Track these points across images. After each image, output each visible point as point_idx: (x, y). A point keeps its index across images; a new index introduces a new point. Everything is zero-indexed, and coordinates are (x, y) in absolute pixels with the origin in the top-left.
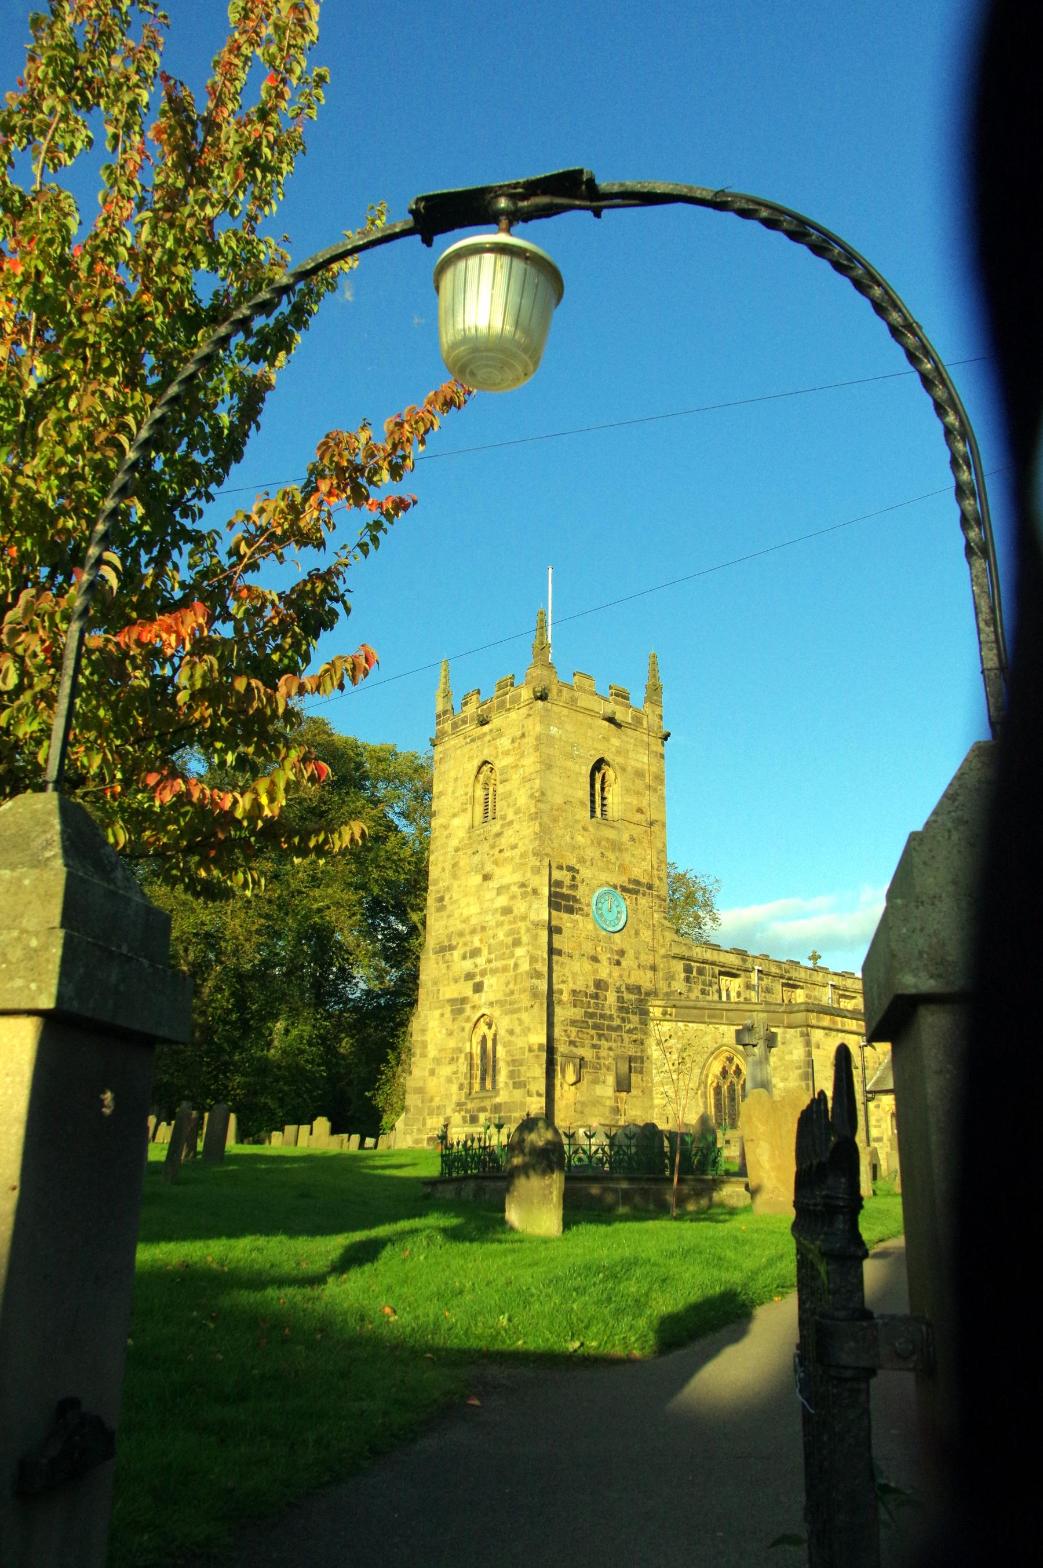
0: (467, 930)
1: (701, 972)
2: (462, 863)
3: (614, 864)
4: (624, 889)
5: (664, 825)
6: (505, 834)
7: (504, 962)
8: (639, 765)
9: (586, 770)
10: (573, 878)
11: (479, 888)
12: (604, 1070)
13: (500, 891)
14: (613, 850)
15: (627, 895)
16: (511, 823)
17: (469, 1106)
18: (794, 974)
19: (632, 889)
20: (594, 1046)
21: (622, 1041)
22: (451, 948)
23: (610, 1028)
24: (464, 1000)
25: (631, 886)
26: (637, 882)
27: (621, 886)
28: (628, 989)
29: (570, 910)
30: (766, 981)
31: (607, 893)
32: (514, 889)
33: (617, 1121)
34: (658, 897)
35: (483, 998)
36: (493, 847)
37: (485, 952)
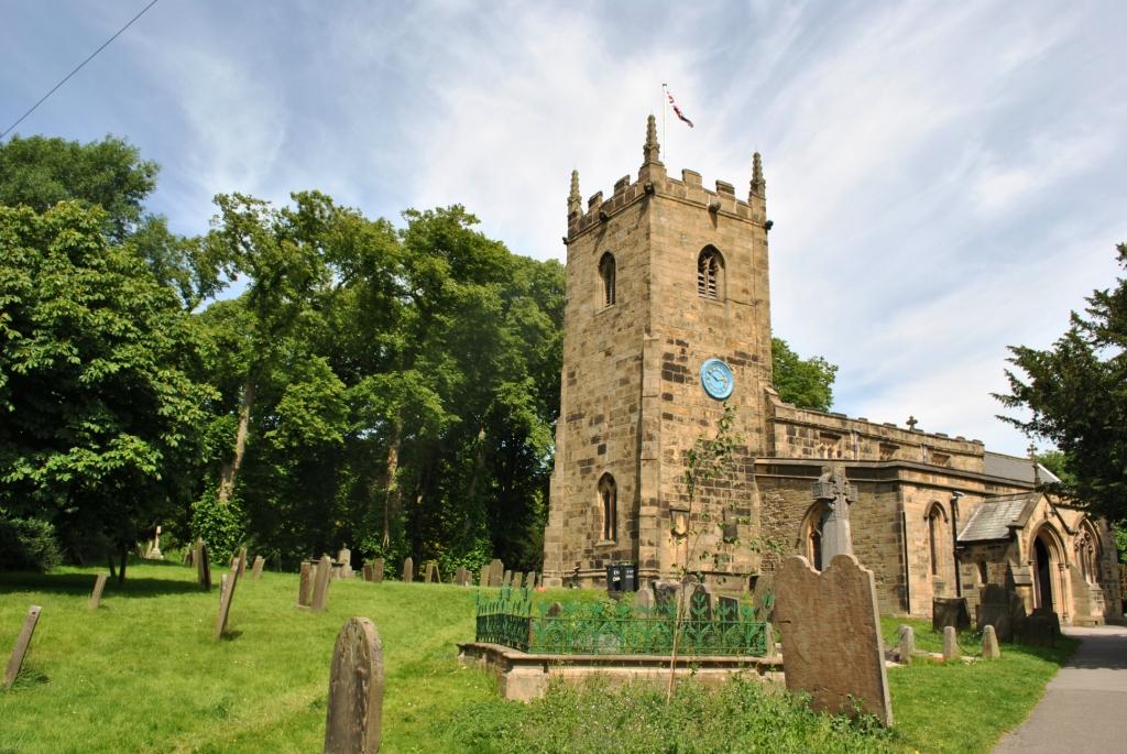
0: (594, 400)
1: (803, 434)
2: (589, 344)
3: (722, 339)
4: (731, 361)
5: (768, 304)
6: (623, 315)
7: (623, 426)
8: (744, 251)
9: (694, 256)
10: (683, 351)
11: (601, 364)
12: (713, 522)
13: (619, 364)
14: (721, 327)
15: (733, 366)
16: (627, 305)
17: (595, 553)
18: (891, 436)
19: (739, 360)
20: (703, 500)
21: (730, 495)
22: (581, 416)
23: (718, 484)
24: (591, 461)
25: (737, 358)
26: (742, 354)
27: (728, 358)
29: (680, 380)
30: (865, 442)
31: (716, 363)
32: (631, 363)
33: (726, 567)
34: (763, 367)
35: (607, 458)
36: (613, 326)
37: (607, 418)
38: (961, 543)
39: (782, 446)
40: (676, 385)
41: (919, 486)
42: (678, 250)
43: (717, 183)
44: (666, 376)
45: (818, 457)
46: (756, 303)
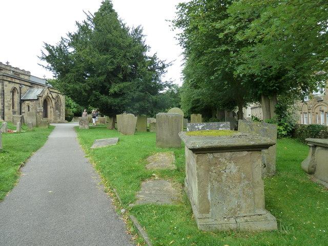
41: (10, 82)
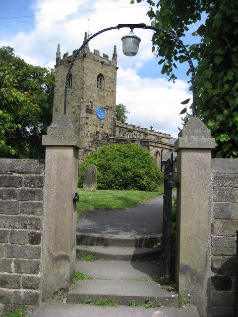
9: (96, 76)
18: (146, 132)
20: (95, 148)
26: (108, 107)
28: (105, 134)
29: (91, 113)
32: (76, 107)
38: (163, 162)
39: (117, 133)
40: (89, 115)
41: (154, 146)
42: (92, 75)
43: (104, 54)
44: (87, 112)
45: (126, 137)
46: (113, 91)
